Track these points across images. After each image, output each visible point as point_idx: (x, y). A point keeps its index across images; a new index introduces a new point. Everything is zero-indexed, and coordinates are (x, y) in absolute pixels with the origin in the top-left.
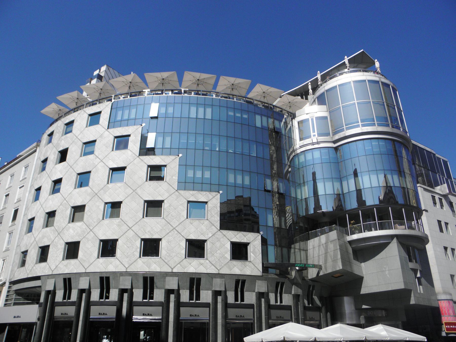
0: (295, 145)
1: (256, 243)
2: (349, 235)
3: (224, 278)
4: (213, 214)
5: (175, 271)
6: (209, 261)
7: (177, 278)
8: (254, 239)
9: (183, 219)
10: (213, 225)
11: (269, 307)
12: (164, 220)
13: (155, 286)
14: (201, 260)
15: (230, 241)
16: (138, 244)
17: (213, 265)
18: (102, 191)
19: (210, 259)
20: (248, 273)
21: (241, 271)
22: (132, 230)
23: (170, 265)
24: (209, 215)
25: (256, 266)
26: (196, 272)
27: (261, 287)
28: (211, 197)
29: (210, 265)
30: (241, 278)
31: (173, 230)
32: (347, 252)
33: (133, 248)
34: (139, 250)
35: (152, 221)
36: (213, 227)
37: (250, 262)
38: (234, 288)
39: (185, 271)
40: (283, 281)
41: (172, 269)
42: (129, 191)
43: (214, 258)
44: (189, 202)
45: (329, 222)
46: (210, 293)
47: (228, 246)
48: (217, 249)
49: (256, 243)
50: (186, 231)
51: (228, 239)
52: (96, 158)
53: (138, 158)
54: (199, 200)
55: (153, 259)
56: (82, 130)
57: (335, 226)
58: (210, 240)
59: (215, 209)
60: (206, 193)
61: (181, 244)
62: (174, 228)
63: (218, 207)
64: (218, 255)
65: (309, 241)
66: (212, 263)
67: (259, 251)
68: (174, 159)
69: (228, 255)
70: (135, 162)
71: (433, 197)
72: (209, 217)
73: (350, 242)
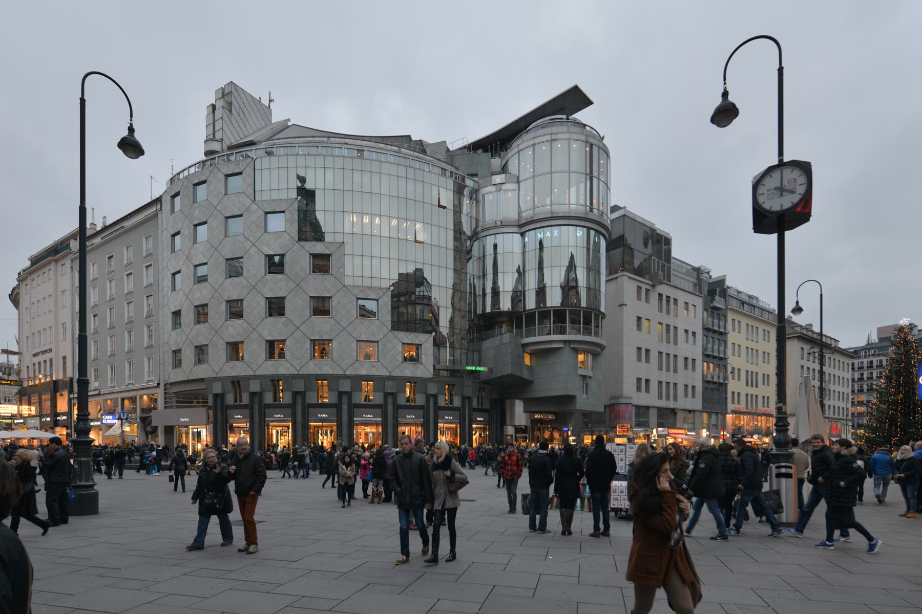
5: (347, 373)
7: (350, 380)
9: (352, 319)
10: (385, 325)
11: (438, 408)
12: (332, 320)
18: (260, 284)
19: (381, 361)
20: (419, 375)
27: (432, 389)
34: (309, 351)
35: (320, 320)
36: (384, 327)
37: (421, 364)
39: (358, 373)
41: (345, 371)
42: (293, 285)
44: (358, 299)
47: (400, 347)
52: (246, 241)
53: (297, 244)
56: (221, 198)
61: (352, 345)
62: (344, 329)
68: (339, 247)
70: (295, 248)
73: (524, 346)
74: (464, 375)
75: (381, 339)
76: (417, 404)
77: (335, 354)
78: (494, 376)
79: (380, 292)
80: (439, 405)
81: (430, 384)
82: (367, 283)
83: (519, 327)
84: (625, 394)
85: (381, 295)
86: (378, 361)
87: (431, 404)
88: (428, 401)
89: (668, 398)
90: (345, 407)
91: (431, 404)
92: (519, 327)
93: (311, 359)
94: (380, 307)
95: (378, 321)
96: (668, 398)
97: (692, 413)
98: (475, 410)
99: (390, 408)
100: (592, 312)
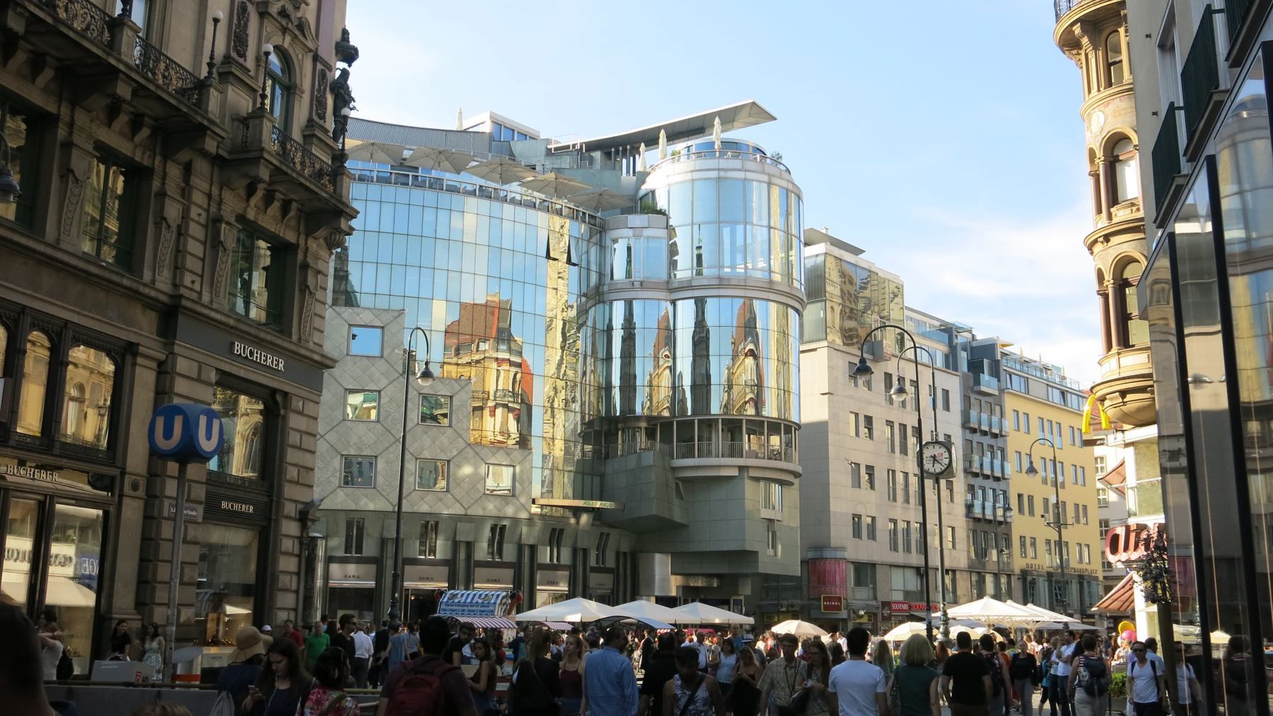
2: (673, 458)
13: (365, 532)
16: (337, 463)
19: (454, 491)
22: (326, 440)
23: (391, 500)
28: (457, 387)
31: (394, 443)
33: (328, 470)
34: (338, 474)
36: (460, 439)
39: (415, 509)
50: (416, 445)
55: (362, 490)
64: (466, 485)
65: (608, 461)
73: (674, 469)
75: (454, 457)
76: (504, 560)
77: (380, 479)
83: (667, 439)
84: (834, 542)
89: (908, 549)
90: (389, 563)
92: (667, 439)
93: (340, 487)
94: (454, 408)
96: (908, 549)
98: (594, 570)
100: (780, 424)
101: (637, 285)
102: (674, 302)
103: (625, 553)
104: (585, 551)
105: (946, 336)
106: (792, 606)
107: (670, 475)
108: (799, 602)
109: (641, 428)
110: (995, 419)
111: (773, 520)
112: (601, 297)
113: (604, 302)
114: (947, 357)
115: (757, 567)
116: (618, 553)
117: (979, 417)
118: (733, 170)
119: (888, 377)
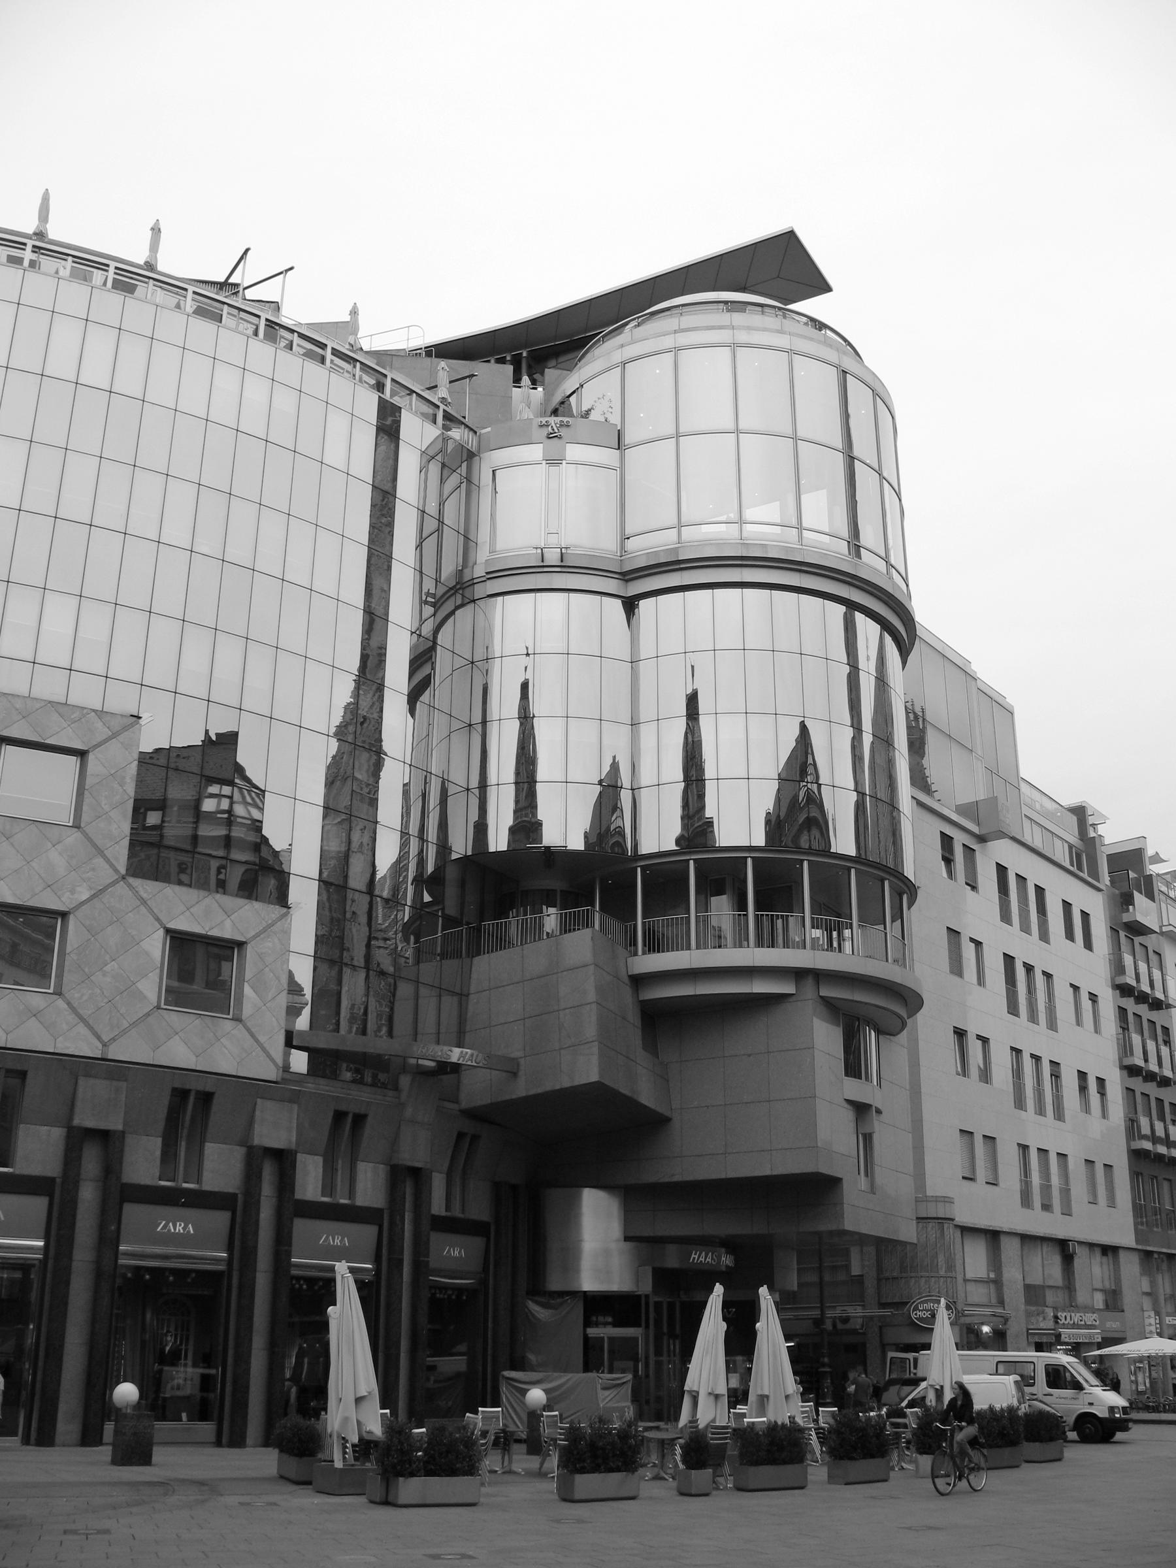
0: (470, 564)
1: (270, 944)
2: (636, 954)
3: (126, 1080)
4: (107, 808)
6: (69, 1003)
8: (264, 930)
10: (101, 853)
14: (35, 998)
15: (168, 931)
17: (82, 1019)
20: (226, 1066)
21: (197, 1056)
24: (85, 808)
25: (262, 1039)
26: (9, 1046)
29: (71, 1018)
30: (195, 1085)
32: (624, 1018)
36: (99, 861)
37: (238, 1019)
38: (161, 1125)
40: (363, 1112)
43: (90, 992)
45: (561, 891)
46: (57, 1134)
47: (155, 946)
48: (107, 958)
49: (270, 944)
51: (158, 919)
54: (48, 741)
57: (588, 910)
58: (79, 913)
59: (116, 786)
60: (84, 716)
63: (128, 780)
64: (109, 979)
65: (476, 960)
66: (81, 1012)
67: (278, 978)
69: (151, 987)
71: (947, 841)
72: (85, 818)
73: (639, 981)
74: (405, 1081)
78: (521, 1089)
79: (99, 725)
80: (298, 1195)
81: (269, 1104)
82: (49, 687)
85: (99, 739)
86: (58, 993)
87: (267, 1190)
88: (251, 1175)
91: (267, 1190)
94: (89, 781)
95: (76, 835)
97: (1110, 1254)
99: (88, 1194)
101: (552, 557)
102: (630, 605)
103: (514, 1187)
104: (416, 1174)
105: (1073, 820)
106: (846, 1320)
107: (627, 991)
108: (859, 1309)
109: (556, 890)
110: (1157, 974)
111: (871, 1106)
112: (468, 593)
113: (474, 601)
114: (1076, 856)
115: (840, 1216)
116: (497, 1186)
117: (1136, 970)
118: (765, 330)
119: (1002, 870)
